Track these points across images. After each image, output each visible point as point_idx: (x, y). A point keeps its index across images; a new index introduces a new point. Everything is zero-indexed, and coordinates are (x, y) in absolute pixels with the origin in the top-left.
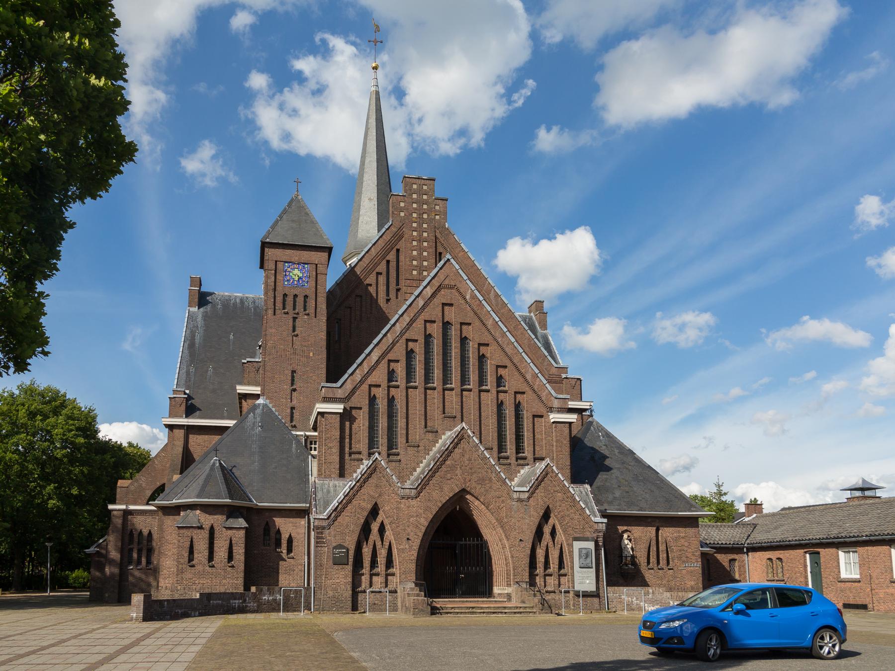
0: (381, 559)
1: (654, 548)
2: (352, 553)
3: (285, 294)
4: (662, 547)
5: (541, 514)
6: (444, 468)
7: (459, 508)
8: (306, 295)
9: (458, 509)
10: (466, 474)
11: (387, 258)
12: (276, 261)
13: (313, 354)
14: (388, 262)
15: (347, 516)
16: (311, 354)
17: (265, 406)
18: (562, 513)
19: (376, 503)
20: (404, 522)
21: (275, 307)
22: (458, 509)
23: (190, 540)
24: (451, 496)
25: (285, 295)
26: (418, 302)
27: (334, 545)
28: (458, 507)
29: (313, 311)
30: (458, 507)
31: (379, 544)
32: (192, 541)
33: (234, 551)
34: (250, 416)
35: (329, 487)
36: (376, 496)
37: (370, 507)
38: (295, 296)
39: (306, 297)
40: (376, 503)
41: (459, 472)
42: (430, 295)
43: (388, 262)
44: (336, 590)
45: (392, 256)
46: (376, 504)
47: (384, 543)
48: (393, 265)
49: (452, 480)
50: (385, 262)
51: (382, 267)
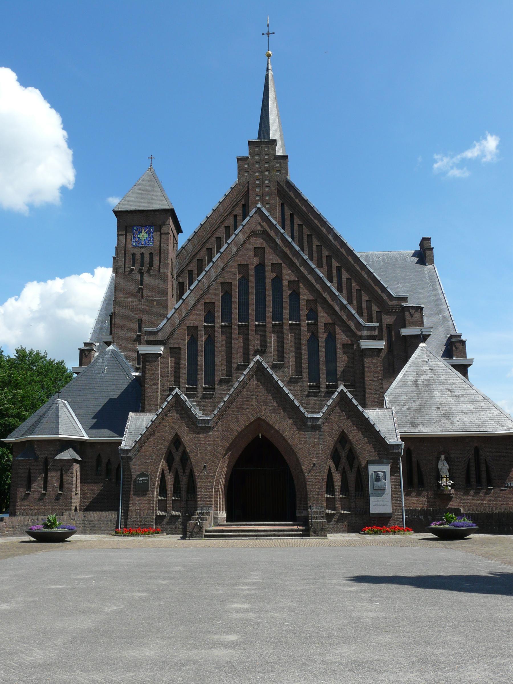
1: (473, 469)
3: (134, 253)
4: (483, 467)
5: (336, 439)
6: (240, 399)
7: (262, 435)
8: (151, 253)
9: (260, 437)
10: (261, 403)
11: (235, 213)
12: (126, 227)
13: (157, 303)
14: (235, 216)
15: (150, 447)
16: (155, 304)
17: (113, 351)
18: (357, 437)
19: (177, 433)
20: (202, 451)
21: (125, 266)
22: (260, 437)
23: (28, 471)
24: (247, 425)
25: (134, 255)
26: (231, 248)
27: (138, 473)
28: (260, 435)
30: (260, 435)
31: (180, 471)
32: (29, 473)
33: (64, 481)
34: (99, 361)
35: (143, 421)
36: (177, 427)
37: (171, 437)
38: (142, 254)
39: (151, 254)
40: (177, 433)
41: (254, 402)
42: (242, 240)
43: (235, 216)
44: (139, 514)
46: (177, 434)
47: (186, 471)
49: (248, 410)
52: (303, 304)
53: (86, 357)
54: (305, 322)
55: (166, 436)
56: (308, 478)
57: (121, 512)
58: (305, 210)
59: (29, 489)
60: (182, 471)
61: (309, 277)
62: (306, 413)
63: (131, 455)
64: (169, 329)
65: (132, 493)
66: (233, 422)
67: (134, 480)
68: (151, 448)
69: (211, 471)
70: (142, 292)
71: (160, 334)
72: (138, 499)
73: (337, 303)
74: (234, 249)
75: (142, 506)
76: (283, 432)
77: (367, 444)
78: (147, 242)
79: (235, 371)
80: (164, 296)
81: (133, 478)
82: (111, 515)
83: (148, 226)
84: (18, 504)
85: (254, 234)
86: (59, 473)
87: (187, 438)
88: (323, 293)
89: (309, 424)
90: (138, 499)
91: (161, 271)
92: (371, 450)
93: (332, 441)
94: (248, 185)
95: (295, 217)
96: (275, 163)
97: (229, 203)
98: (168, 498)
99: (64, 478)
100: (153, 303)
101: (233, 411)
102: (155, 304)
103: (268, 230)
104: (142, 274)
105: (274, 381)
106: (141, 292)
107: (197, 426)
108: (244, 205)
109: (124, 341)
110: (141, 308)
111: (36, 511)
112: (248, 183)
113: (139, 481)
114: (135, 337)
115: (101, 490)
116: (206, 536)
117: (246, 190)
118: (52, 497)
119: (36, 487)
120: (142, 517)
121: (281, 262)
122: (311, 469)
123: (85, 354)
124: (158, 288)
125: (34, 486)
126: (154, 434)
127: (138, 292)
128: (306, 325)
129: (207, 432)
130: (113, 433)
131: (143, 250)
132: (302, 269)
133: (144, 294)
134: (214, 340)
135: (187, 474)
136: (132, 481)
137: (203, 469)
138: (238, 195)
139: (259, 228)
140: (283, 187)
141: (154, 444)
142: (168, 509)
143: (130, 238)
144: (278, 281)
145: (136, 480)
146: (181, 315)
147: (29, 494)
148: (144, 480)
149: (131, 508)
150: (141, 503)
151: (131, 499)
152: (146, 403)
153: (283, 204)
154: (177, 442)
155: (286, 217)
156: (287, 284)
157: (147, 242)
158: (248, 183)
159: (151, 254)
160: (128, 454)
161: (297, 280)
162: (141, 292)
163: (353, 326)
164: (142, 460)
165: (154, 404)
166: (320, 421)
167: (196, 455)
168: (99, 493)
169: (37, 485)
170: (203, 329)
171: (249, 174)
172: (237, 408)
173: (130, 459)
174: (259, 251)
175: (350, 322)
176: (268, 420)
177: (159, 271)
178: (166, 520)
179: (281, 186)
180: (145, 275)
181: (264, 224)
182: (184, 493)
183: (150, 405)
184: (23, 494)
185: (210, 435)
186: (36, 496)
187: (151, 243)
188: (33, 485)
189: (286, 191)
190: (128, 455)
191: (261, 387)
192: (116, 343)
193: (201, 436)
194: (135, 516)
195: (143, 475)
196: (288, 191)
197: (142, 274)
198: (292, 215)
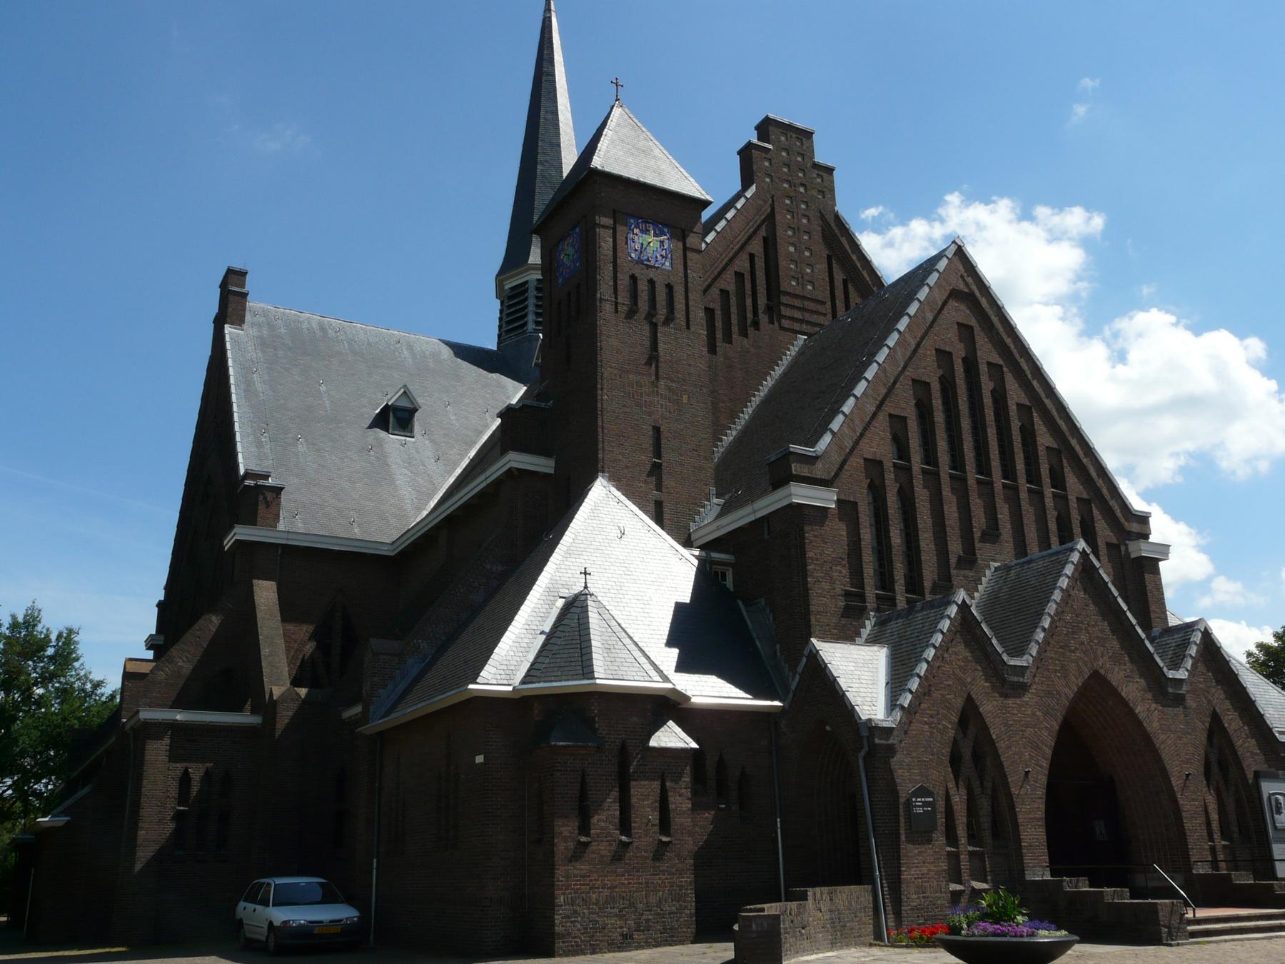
0: (985, 821)
2: (941, 805)
13: (689, 397)
14: (752, 256)
29: (683, 318)
31: (976, 784)
32: (583, 783)
33: (672, 807)
36: (969, 680)
39: (669, 287)
45: (756, 247)
48: (760, 263)
50: (748, 257)
51: (742, 264)
52: (1042, 452)
53: (268, 506)
54: (1049, 491)
55: (951, 699)
56: (1183, 804)
57: (882, 887)
58: (868, 279)
59: (584, 828)
60: (978, 782)
61: (1047, 402)
62: (1165, 669)
63: (895, 742)
64: (837, 459)
65: (903, 837)
66: (1058, 677)
67: (905, 804)
68: (927, 727)
69: (1037, 785)
70: (657, 367)
71: (819, 465)
72: (917, 851)
73: (1091, 460)
74: (930, 317)
75: (925, 870)
76: (1134, 704)
77: (1249, 740)
78: (659, 258)
79: (955, 569)
80: (701, 386)
81: (902, 800)
82: (853, 897)
83: (661, 224)
84: (560, 873)
85: (955, 294)
86: (656, 785)
87: (989, 707)
88: (1070, 438)
89: (1170, 690)
90: (917, 851)
91: (692, 329)
92: (1255, 751)
93: (1203, 729)
94: (773, 201)
95: (850, 286)
96: (815, 176)
97: (743, 227)
98: (962, 848)
99: (671, 799)
100: (682, 397)
101: (1056, 653)
102: (685, 397)
103: (978, 294)
104: (654, 327)
105: (1111, 596)
106: (653, 366)
107: (1004, 680)
108: (765, 239)
109: (626, 471)
110: (658, 401)
111: (606, 892)
112: (772, 197)
113: (916, 806)
114: (648, 467)
115: (709, 835)
116: (1194, 934)
117: (769, 210)
118: (646, 851)
119: (603, 824)
120: (928, 897)
121: (1001, 362)
122: (1184, 785)
123: (265, 498)
124: (690, 365)
125: (599, 821)
126: (929, 695)
127: (649, 363)
128: (1051, 495)
129: (1020, 696)
130: (738, 690)
131: (651, 274)
132: (1035, 383)
133: (661, 373)
134: (914, 499)
135: (989, 792)
136: (901, 807)
137: (1024, 780)
138: (755, 215)
139: (962, 287)
140: (830, 225)
141: (931, 716)
142: (965, 877)
143: (624, 239)
144: (1000, 398)
145: (908, 804)
146: (855, 431)
147: (586, 844)
148: (925, 804)
149: (907, 874)
150: (924, 862)
151: (903, 852)
152: (813, 619)
153: (829, 258)
154: (969, 716)
155: (836, 283)
156: (1014, 407)
157: (659, 258)
158: (772, 197)
159: (669, 287)
160: (888, 740)
161: (1028, 404)
162: (653, 366)
163: (1119, 511)
164: (914, 754)
165: (828, 625)
166: (1185, 688)
167: (1009, 747)
168: (705, 841)
169: (605, 819)
170: (892, 469)
171: (772, 181)
172: (1061, 647)
173: (891, 750)
174: (965, 331)
175: (1113, 501)
176: (1109, 677)
177: (688, 327)
178: (964, 900)
179: (828, 223)
180: (660, 329)
181: (969, 280)
182: (987, 835)
183: (821, 626)
184: (571, 845)
185: (1027, 703)
186: (602, 848)
187: (667, 264)
188: (594, 820)
189: (836, 234)
190: (890, 742)
191: (1092, 607)
192: (609, 472)
193: (1010, 702)
194: (914, 896)
195: (922, 792)
196: (839, 235)
197: (654, 327)
198: (845, 282)
